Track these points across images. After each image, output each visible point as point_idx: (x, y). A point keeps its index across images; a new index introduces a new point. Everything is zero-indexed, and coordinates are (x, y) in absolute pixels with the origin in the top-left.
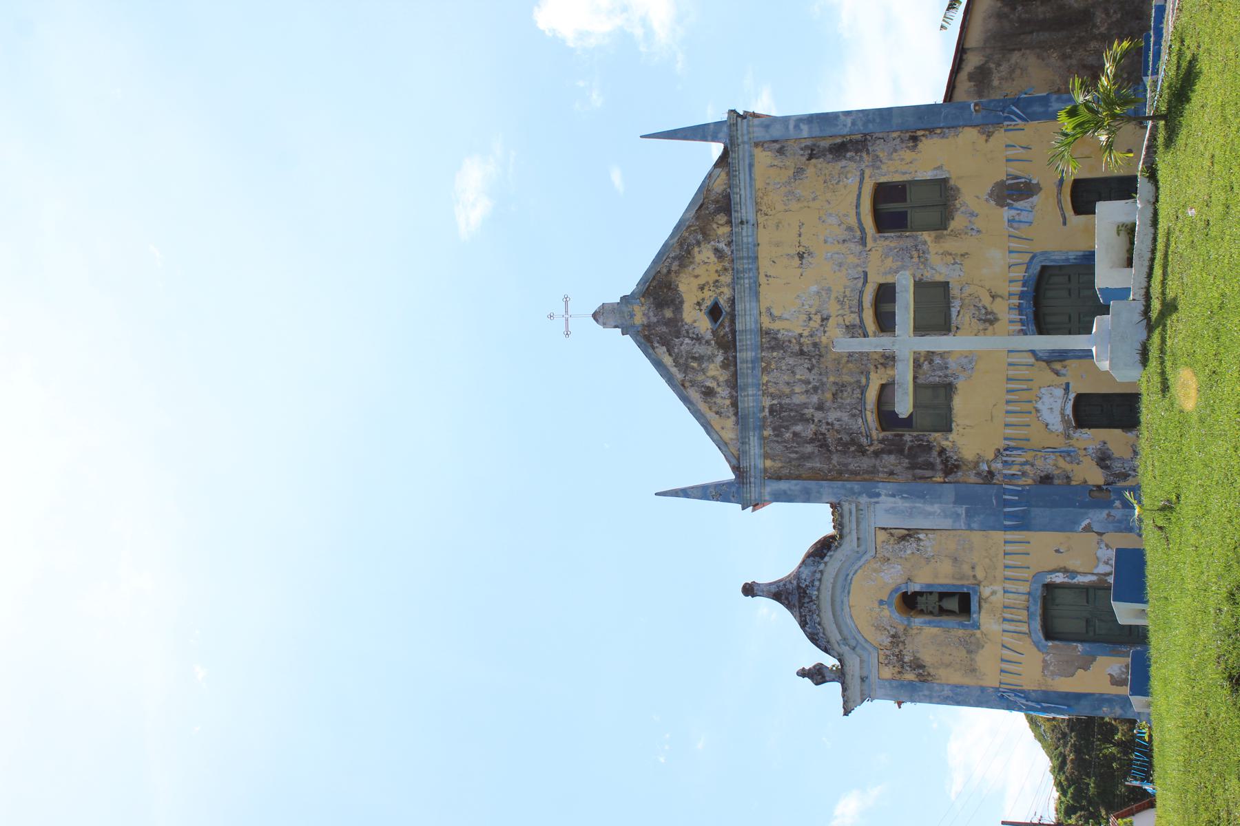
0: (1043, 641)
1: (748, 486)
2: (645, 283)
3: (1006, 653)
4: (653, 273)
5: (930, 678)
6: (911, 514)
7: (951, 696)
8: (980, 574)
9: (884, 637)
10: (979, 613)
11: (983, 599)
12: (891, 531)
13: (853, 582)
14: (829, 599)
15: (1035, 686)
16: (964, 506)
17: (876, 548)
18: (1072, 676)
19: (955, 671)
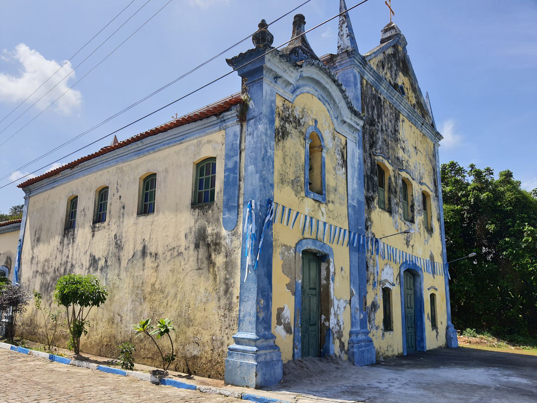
0: (302, 250)
1: (360, 61)
2: (408, 61)
3: (293, 214)
4: (410, 68)
5: (277, 140)
6: (353, 167)
7: (267, 154)
8: (330, 205)
9: (298, 113)
10: (313, 199)
11: (320, 204)
12: (345, 149)
13: (323, 106)
14: (322, 81)
15: (275, 236)
16: (357, 205)
17: (339, 133)
18: (283, 272)
19: (281, 165)
